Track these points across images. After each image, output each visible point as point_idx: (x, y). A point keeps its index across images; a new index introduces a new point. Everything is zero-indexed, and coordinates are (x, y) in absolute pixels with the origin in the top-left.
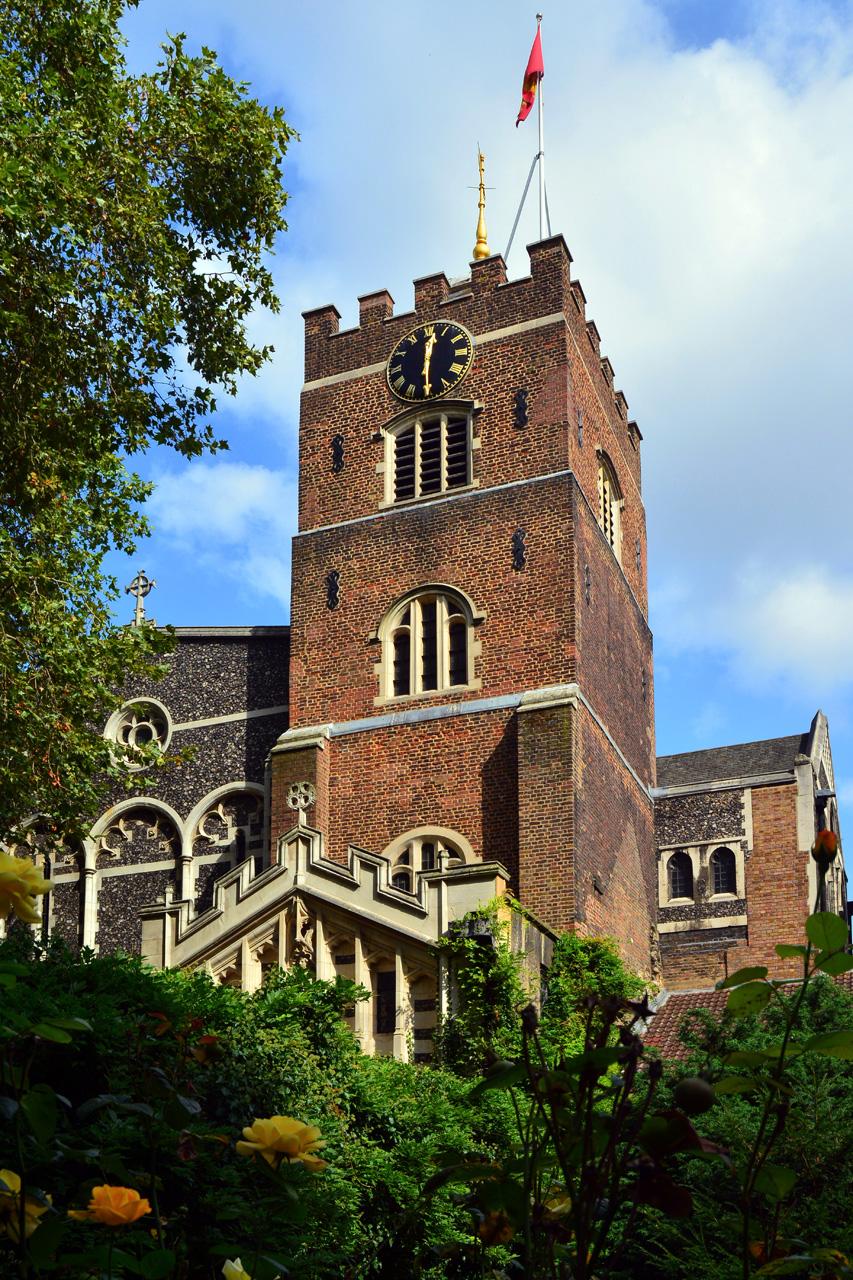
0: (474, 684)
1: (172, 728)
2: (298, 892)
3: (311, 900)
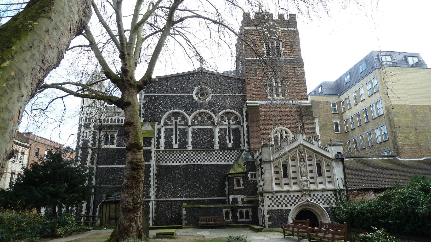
1: (211, 95)
2: (302, 144)
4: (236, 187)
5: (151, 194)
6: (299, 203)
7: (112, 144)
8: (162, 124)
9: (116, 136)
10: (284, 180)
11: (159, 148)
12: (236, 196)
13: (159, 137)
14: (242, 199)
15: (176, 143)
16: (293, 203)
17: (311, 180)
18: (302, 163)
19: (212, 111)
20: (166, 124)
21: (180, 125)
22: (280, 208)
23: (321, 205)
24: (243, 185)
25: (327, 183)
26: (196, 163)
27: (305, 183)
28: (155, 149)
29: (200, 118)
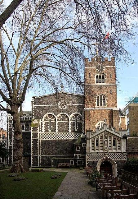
0: (106, 106)
1: (67, 105)
3: (107, 131)
4: (77, 150)
5: (38, 153)
6: (103, 158)
7: (23, 130)
8: (43, 120)
9: (24, 126)
10: (96, 147)
11: (42, 132)
12: (76, 154)
13: (42, 127)
14: (79, 156)
15: (50, 129)
16: (99, 158)
17: (110, 148)
18: (105, 140)
19: (67, 113)
20: (45, 120)
21: (52, 121)
22: (93, 160)
23: (113, 160)
24: (80, 149)
25: (117, 149)
26: (59, 139)
27: (106, 149)
28: (40, 132)
29: (61, 117)
